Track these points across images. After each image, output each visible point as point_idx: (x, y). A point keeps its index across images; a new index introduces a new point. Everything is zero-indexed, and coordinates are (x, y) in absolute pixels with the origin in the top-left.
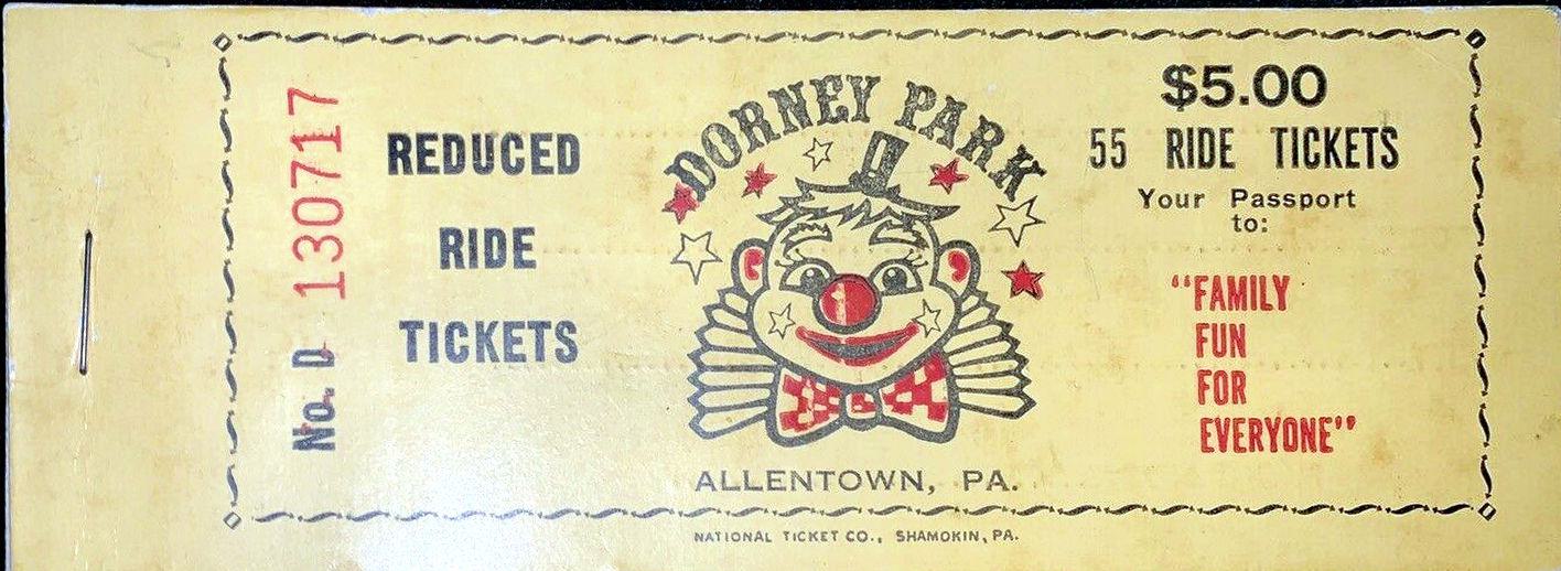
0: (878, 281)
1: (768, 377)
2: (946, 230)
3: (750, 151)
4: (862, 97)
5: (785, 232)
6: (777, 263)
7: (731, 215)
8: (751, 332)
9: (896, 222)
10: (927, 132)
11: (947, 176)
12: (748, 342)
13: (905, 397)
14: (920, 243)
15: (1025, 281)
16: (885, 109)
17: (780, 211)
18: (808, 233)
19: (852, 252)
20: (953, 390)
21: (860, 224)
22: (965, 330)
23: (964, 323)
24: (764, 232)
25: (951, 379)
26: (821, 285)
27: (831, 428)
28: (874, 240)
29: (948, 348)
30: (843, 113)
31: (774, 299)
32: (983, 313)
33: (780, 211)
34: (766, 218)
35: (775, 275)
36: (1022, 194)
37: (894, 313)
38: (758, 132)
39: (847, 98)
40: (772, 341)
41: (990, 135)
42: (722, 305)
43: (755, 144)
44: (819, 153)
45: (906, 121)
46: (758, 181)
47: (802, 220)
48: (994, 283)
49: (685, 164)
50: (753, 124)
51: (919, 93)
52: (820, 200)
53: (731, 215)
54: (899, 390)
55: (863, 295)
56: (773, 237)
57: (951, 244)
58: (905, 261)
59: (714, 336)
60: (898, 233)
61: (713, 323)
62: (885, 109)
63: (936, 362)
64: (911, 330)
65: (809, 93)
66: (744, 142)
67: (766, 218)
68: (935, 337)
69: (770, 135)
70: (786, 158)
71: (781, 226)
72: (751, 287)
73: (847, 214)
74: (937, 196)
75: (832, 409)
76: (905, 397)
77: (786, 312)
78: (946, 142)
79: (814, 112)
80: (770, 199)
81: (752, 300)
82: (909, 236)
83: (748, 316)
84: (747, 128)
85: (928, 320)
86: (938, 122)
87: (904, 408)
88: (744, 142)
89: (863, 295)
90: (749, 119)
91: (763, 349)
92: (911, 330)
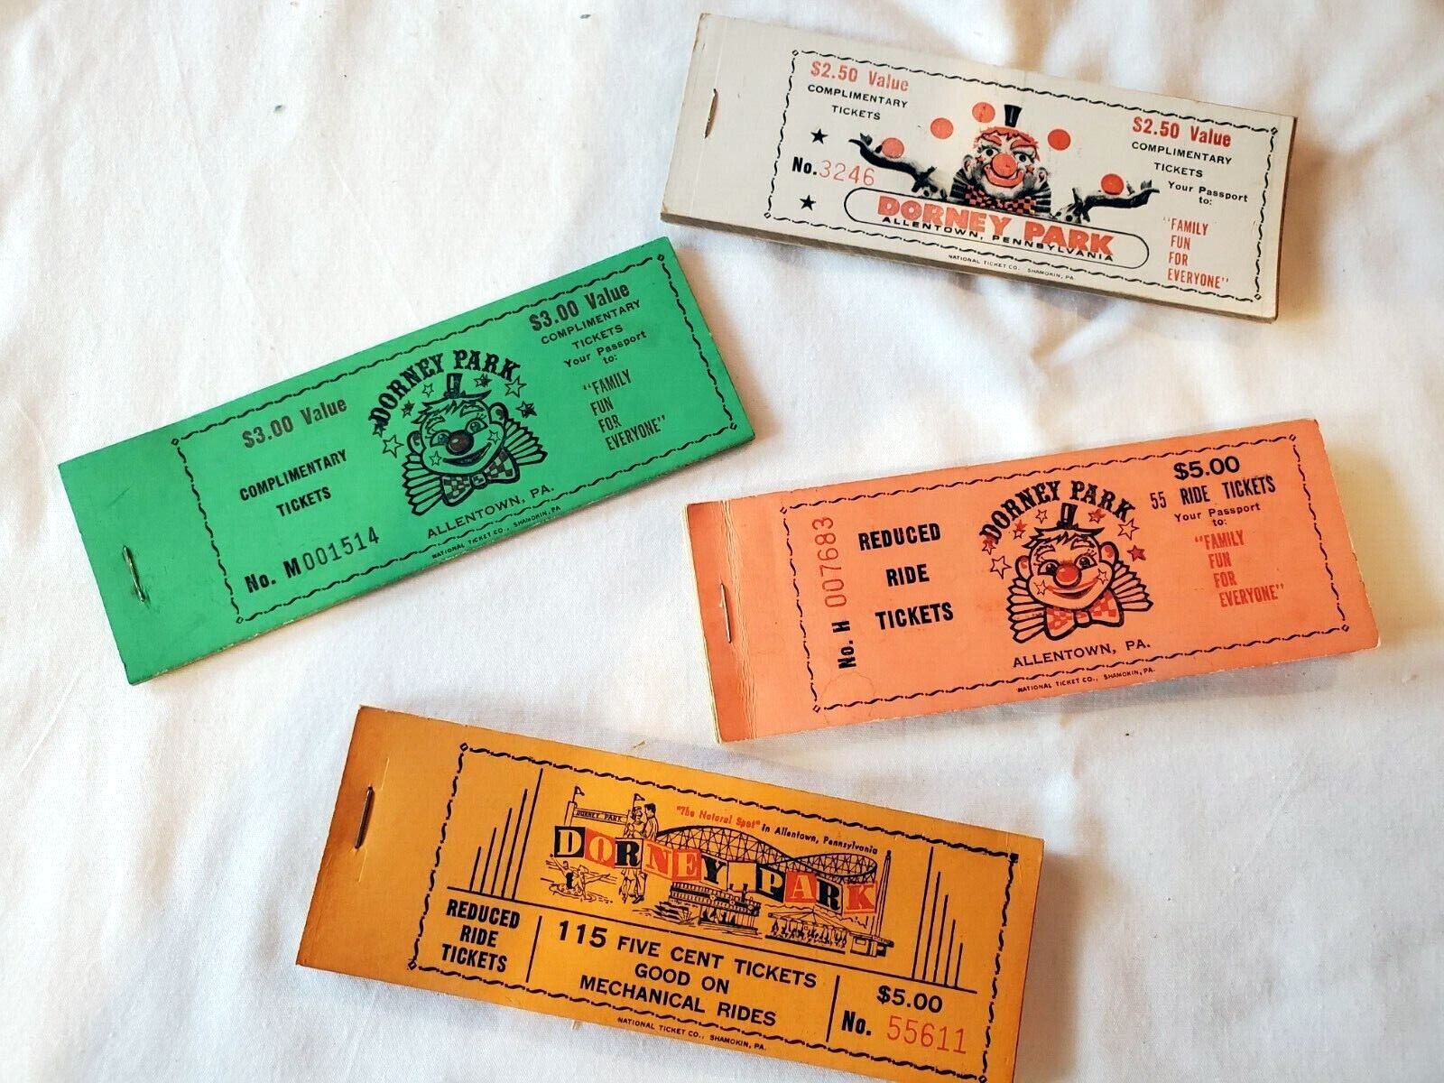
0: (469, 430)
1: (438, 482)
2: (489, 401)
3: (400, 399)
4: (438, 363)
5: (425, 424)
6: (426, 437)
7: (400, 425)
8: (425, 467)
9: (468, 405)
10: (468, 367)
11: (485, 381)
12: (426, 472)
13: (495, 471)
14: (482, 410)
15: (529, 411)
16: (448, 364)
17: (421, 417)
18: (434, 422)
19: (454, 422)
20: (514, 461)
21: (454, 411)
22: (510, 436)
23: (508, 433)
24: (417, 427)
25: (511, 456)
26: (447, 438)
27: (470, 492)
28: (462, 415)
29: (506, 445)
30: (432, 372)
31: (429, 452)
32: (514, 427)
33: (421, 417)
34: (416, 422)
35: (427, 442)
36: (513, 377)
37: (480, 441)
38: (401, 391)
39: (432, 365)
40: (435, 468)
41: (493, 360)
42: (409, 461)
43: (401, 396)
44: (428, 390)
45: (458, 366)
46: (409, 407)
47: (431, 417)
48: (515, 415)
49: (376, 413)
50: (399, 388)
51: (460, 355)
52: (435, 407)
53: (400, 425)
54: (491, 469)
55: (466, 437)
56: (421, 428)
57: (493, 406)
58: (476, 419)
59: (410, 475)
60: (470, 409)
61: (408, 470)
62: (448, 364)
63: (503, 453)
64: (489, 445)
65: (417, 369)
66: (396, 397)
67: (416, 422)
68: (499, 442)
69: (406, 390)
70: (416, 396)
71: (422, 423)
72: (418, 449)
73: (447, 409)
74: (482, 390)
75: (468, 485)
76: (495, 471)
77: (436, 457)
78: (477, 367)
79: (420, 375)
80: (415, 414)
81: (421, 455)
82: (475, 409)
83: (421, 462)
84: (396, 391)
85: (494, 437)
86: (471, 362)
87: (496, 475)
88: (396, 397)
89: (466, 437)
90: (396, 387)
91: (432, 472)
92: (489, 445)
